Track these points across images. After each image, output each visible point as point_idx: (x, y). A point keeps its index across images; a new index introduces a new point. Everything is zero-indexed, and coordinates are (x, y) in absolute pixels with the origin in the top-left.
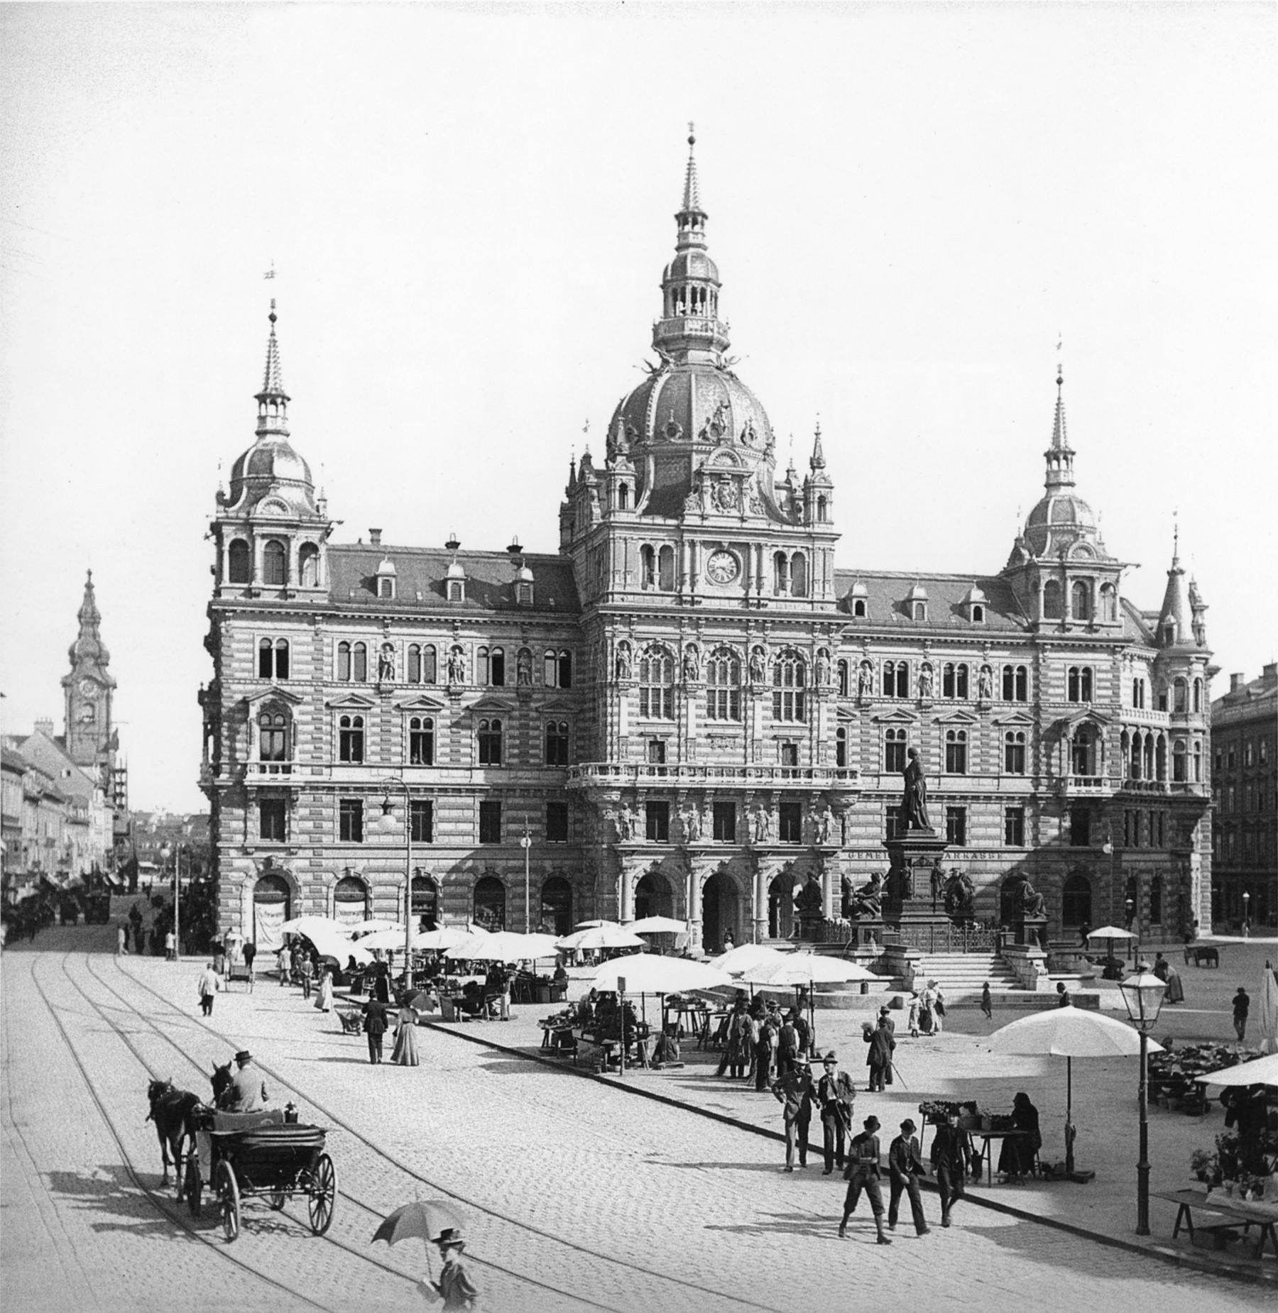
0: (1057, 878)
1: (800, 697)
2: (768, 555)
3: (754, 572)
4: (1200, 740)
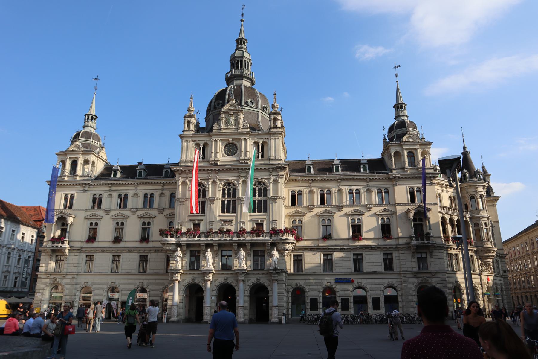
0: (412, 286)
1: (265, 202)
2: (250, 142)
3: (243, 150)
4: (487, 222)
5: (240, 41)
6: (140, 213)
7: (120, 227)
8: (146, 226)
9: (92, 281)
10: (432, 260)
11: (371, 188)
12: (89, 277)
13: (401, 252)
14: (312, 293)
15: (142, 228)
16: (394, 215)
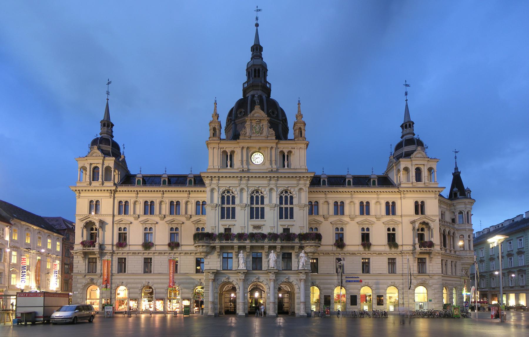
5: (257, 49)
6: (168, 218)
7: (148, 233)
8: (174, 232)
9: (126, 281)
10: (430, 264)
11: (379, 200)
12: (123, 277)
13: (404, 257)
14: (326, 291)
15: (171, 233)
16: (400, 226)
